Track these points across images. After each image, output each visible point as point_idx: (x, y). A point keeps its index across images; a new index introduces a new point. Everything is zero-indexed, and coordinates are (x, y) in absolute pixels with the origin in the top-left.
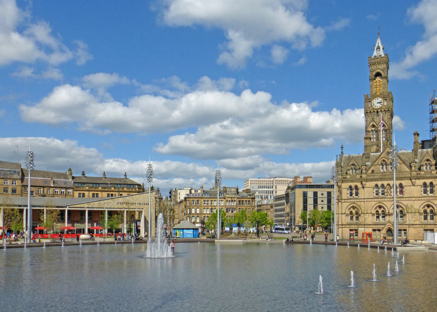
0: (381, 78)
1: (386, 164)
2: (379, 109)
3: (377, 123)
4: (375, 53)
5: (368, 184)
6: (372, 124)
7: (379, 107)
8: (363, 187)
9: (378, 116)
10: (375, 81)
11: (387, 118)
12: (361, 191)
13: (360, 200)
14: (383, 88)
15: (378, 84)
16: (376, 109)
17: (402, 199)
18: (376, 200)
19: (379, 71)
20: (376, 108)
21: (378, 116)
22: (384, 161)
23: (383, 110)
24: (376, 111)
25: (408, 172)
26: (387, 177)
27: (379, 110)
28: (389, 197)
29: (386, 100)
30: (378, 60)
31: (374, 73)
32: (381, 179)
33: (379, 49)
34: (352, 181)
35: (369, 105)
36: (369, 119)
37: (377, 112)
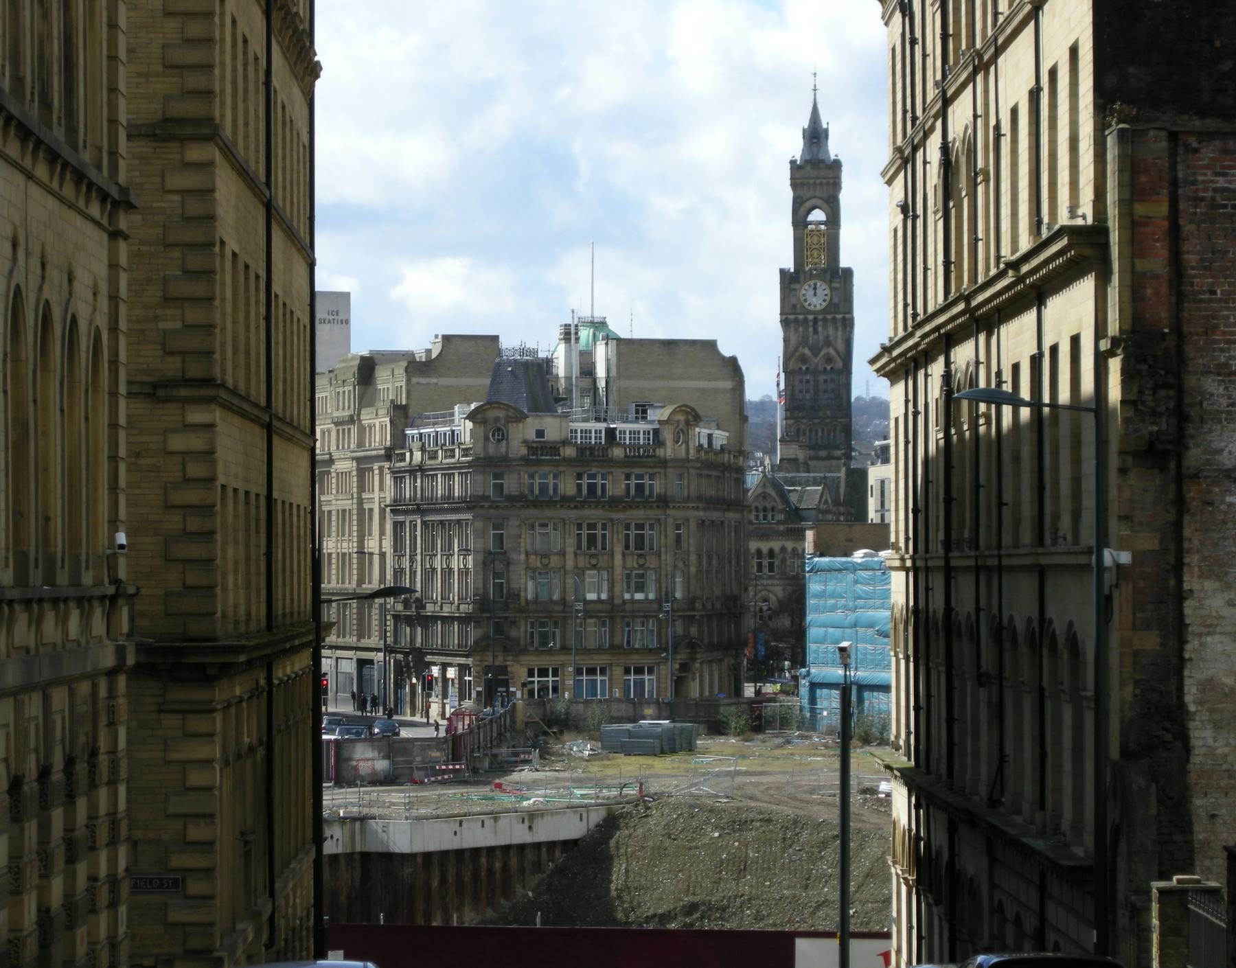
7: (819, 308)
15: (815, 238)
16: (810, 312)
20: (812, 308)
24: (811, 317)
27: (820, 317)
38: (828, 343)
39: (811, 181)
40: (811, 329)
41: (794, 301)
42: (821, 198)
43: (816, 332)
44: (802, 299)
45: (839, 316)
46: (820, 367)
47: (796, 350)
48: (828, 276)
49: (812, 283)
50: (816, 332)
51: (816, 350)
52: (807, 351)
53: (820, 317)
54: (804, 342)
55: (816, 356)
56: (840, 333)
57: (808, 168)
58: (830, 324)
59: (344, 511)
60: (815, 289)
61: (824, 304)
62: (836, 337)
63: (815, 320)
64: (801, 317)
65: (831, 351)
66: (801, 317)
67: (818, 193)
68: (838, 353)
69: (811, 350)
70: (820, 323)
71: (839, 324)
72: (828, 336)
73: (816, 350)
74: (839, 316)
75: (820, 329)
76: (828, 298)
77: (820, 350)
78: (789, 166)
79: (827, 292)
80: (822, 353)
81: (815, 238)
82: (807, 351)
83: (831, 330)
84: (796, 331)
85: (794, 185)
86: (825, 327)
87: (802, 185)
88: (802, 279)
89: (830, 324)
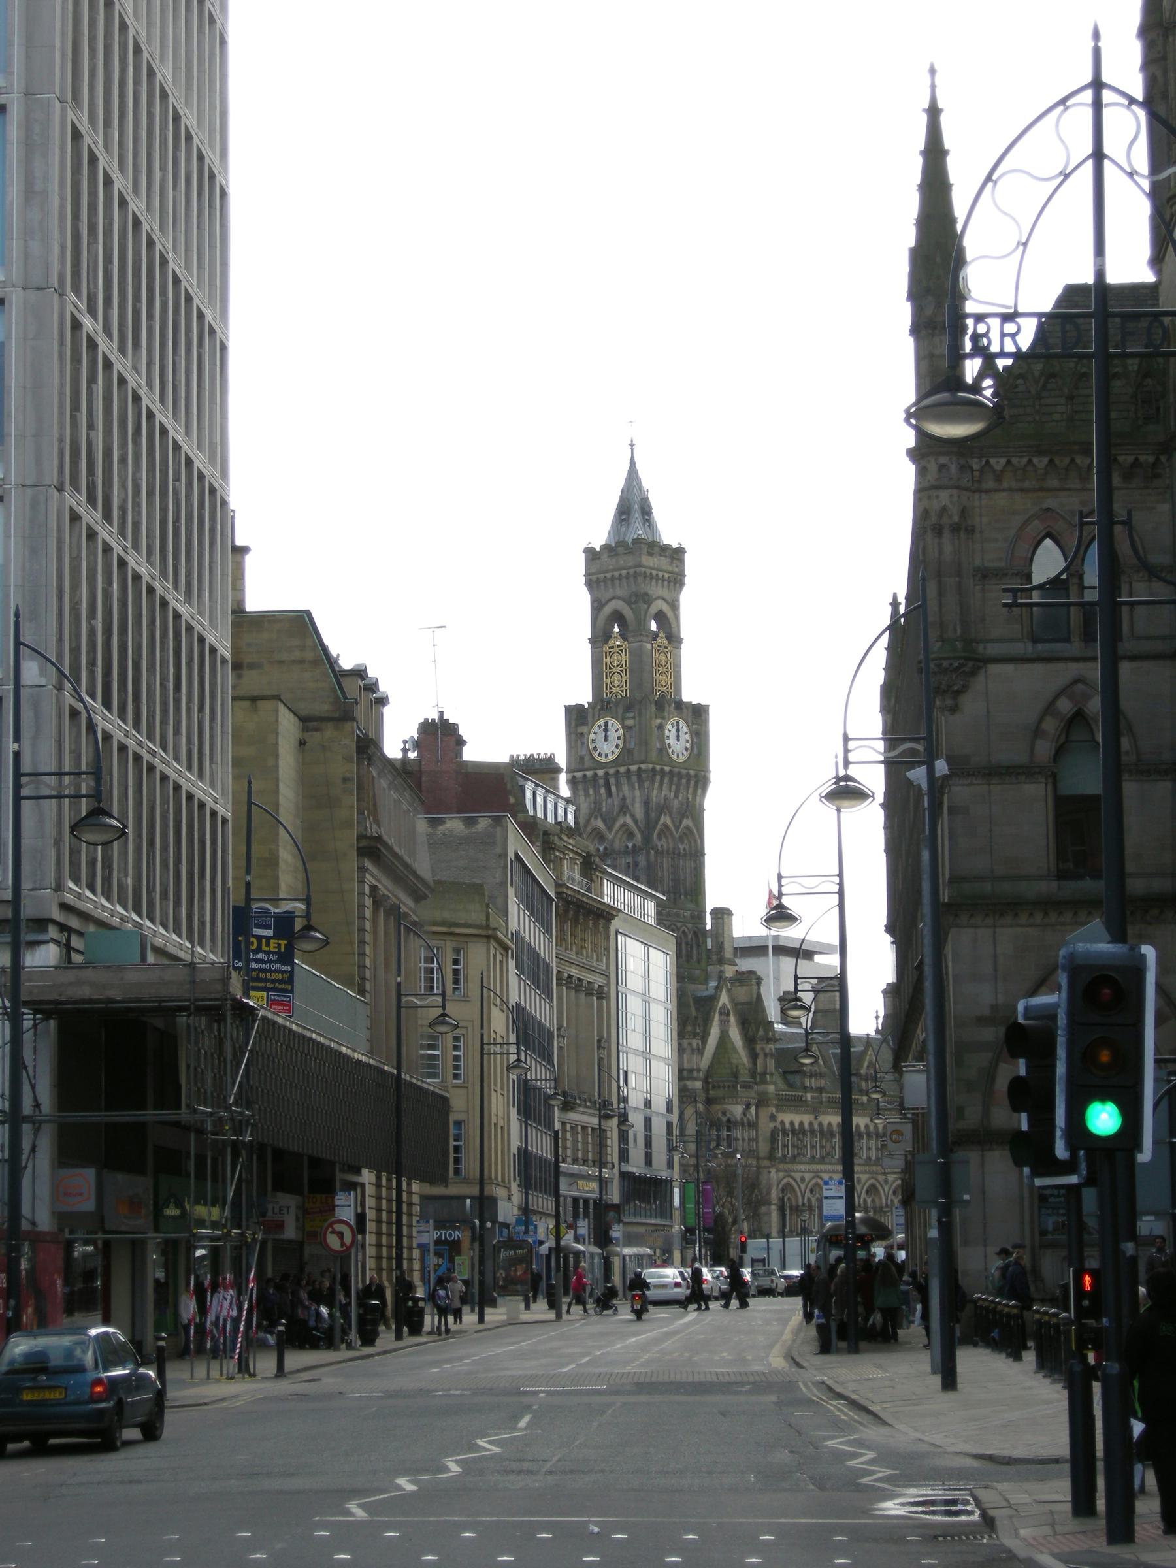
10: (606, 648)
16: (600, 765)
20: (603, 759)
23: (622, 769)
24: (601, 772)
38: (624, 809)
39: (609, 575)
40: (603, 791)
41: (584, 752)
42: (624, 601)
43: (609, 794)
44: (591, 746)
45: (634, 768)
46: (617, 845)
47: (588, 821)
48: (620, 711)
49: (602, 722)
50: (609, 794)
51: (609, 822)
52: (600, 824)
53: (612, 771)
54: (596, 811)
55: (610, 828)
56: (637, 793)
57: (605, 557)
58: (623, 780)
59: (435, 1067)
60: (606, 730)
61: (617, 751)
62: (634, 799)
63: (607, 773)
64: (589, 773)
65: (629, 820)
66: (589, 773)
67: (619, 593)
68: (636, 822)
69: (604, 821)
70: (612, 780)
71: (634, 778)
72: (624, 799)
73: (609, 822)
74: (634, 768)
75: (613, 789)
76: (621, 743)
77: (615, 820)
78: (582, 558)
79: (621, 733)
80: (618, 825)
81: (615, 657)
82: (600, 824)
83: (625, 787)
84: (587, 795)
85: (590, 584)
86: (618, 785)
87: (598, 581)
88: (590, 719)
89: (623, 780)
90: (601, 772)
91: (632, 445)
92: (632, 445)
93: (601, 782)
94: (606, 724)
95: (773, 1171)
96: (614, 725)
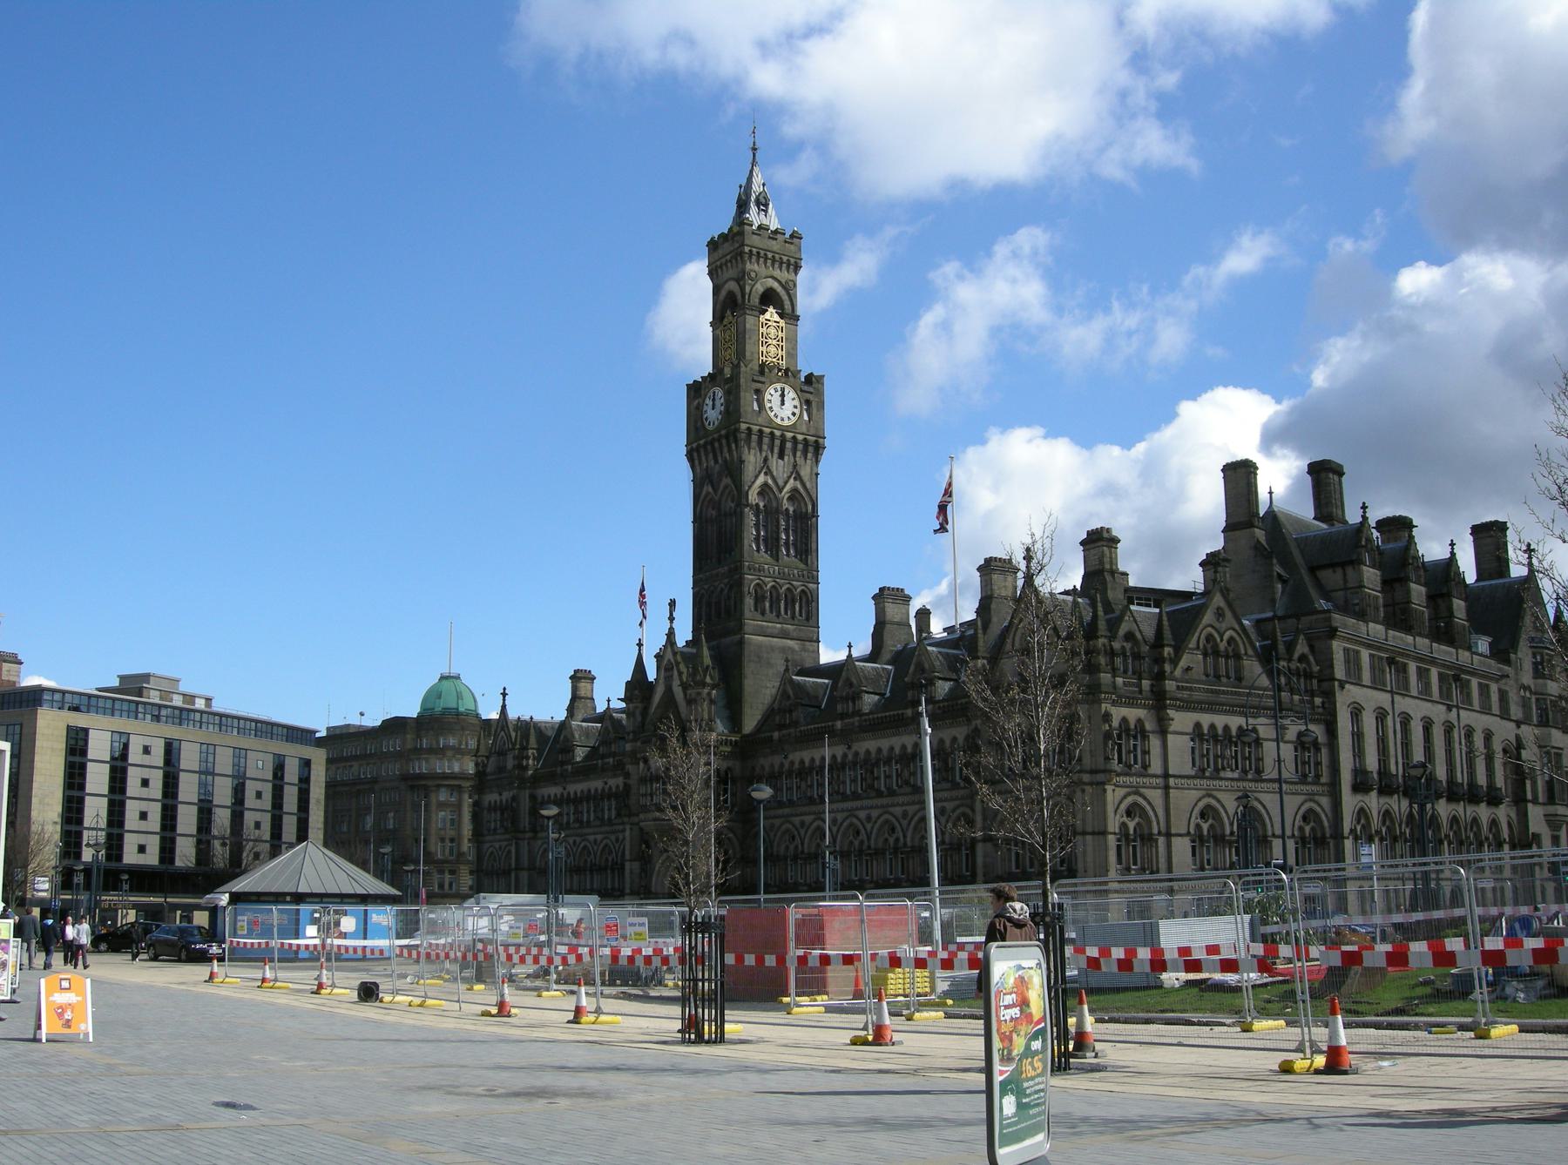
0: (781, 316)
1: (1216, 653)
2: (787, 429)
3: (781, 483)
4: (754, 216)
5: (1181, 721)
6: (761, 479)
7: (786, 423)
8: (1163, 732)
9: (781, 456)
11: (808, 469)
12: (1155, 743)
13: (1154, 781)
14: (788, 353)
15: (772, 331)
16: (780, 427)
17: (1260, 785)
18: (1197, 781)
19: (776, 285)
20: (778, 421)
21: (781, 456)
22: (1209, 638)
23: (800, 437)
25: (1265, 689)
26: (1223, 698)
27: (789, 435)
28: (1229, 774)
29: (808, 402)
30: (775, 246)
31: (759, 288)
32: (1211, 707)
33: (766, 205)
34: (1131, 702)
35: (756, 407)
36: (752, 458)
37: (783, 436)
49: (778, 386)
53: (789, 435)
60: (783, 395)
61: (794, 419)
63: (783, 436)
67: (777, 273)
70: (789, 445)
80: (788, 488)
90: (778, 433)
91: (754, 149)
92: (754, 149)
93: (777, 442)
94: (783, 390)
95: (1109, 788)
96: (790, 394)
